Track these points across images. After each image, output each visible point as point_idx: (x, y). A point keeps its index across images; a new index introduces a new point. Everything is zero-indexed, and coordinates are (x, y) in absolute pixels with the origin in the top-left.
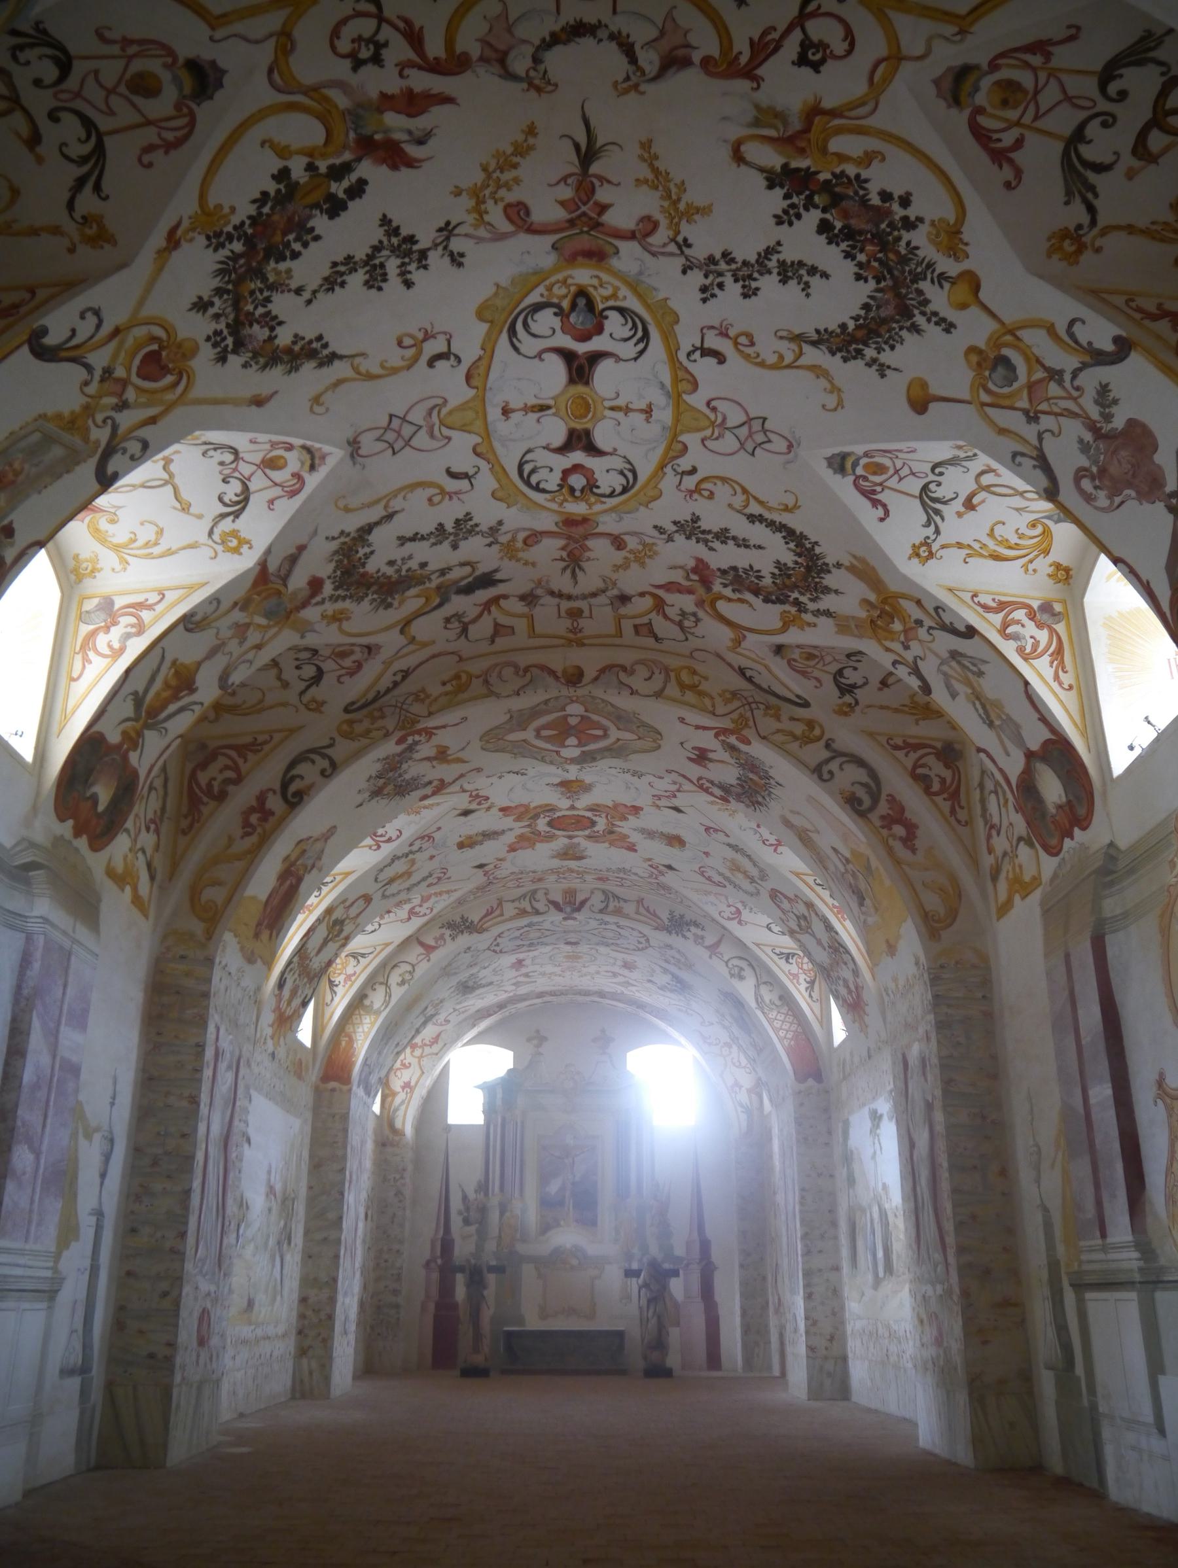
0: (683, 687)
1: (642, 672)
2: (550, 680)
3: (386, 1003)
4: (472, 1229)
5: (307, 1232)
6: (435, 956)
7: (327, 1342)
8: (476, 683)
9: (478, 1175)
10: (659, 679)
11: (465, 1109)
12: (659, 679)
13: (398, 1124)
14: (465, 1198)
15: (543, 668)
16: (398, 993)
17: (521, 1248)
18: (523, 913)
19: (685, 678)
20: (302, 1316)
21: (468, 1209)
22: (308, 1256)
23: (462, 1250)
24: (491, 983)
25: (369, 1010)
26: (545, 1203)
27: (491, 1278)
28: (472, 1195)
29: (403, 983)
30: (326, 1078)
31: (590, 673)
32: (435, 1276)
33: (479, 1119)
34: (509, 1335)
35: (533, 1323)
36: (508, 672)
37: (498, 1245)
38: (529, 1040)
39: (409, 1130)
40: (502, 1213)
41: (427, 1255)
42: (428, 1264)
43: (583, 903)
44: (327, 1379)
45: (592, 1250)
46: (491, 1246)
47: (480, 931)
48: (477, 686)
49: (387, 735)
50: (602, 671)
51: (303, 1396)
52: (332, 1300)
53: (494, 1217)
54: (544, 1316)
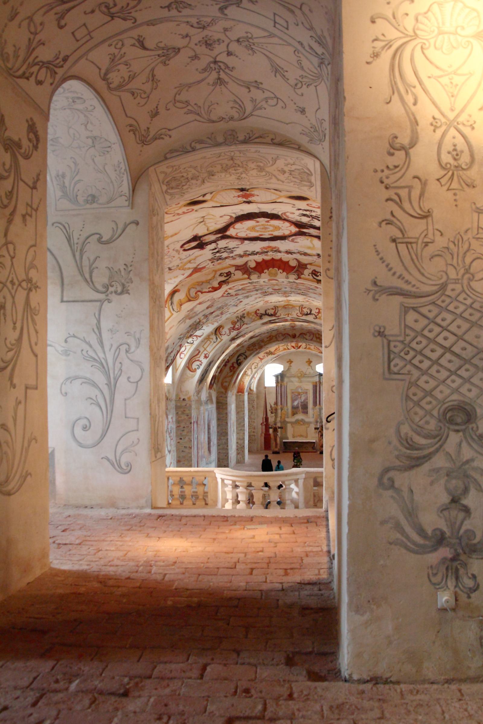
0: (317, 338)
1: (308, 334)
2: (289, 337)
3: (252, 373)
4: (274, 414)
5: (237, 428)
6: (263, 361)
7: (243, 451)
8: (274, 338)
9: (274, 400)
10: (312, 336)
11: (270, 382)
12: (312, 336)
13: (252, 388)
14: (271, 406)
15: (288, 334)
16: (254, 371)
17: (287, 420)
18: (285, 349)
19: (317, 336)
20: (237, 446)
22: (238, 433)
23: (271, 420)
25: (247, 375)
27: (279, 430)
28: (273, 406)
29: (255, 368)
30: (238, 392)
31: (297, 335)
32: (264, 427)
33: (274, 385)
34: (285, 443)
36: (280, 335)
38: (288, 362)
39: (255, 389)
40: (281, 411)
41: (261, 422)
42: (262, 424)
43: (300, 346)
44: (244, 459)
45: (307, 420)
46: (279, 419)
47: (274, 354)
48: (274, 338)
49: (257, 350)
50: (301, 334)
51: (239, 463)
52: (244, 443)
53: (279, 411)
54: (294, 437)
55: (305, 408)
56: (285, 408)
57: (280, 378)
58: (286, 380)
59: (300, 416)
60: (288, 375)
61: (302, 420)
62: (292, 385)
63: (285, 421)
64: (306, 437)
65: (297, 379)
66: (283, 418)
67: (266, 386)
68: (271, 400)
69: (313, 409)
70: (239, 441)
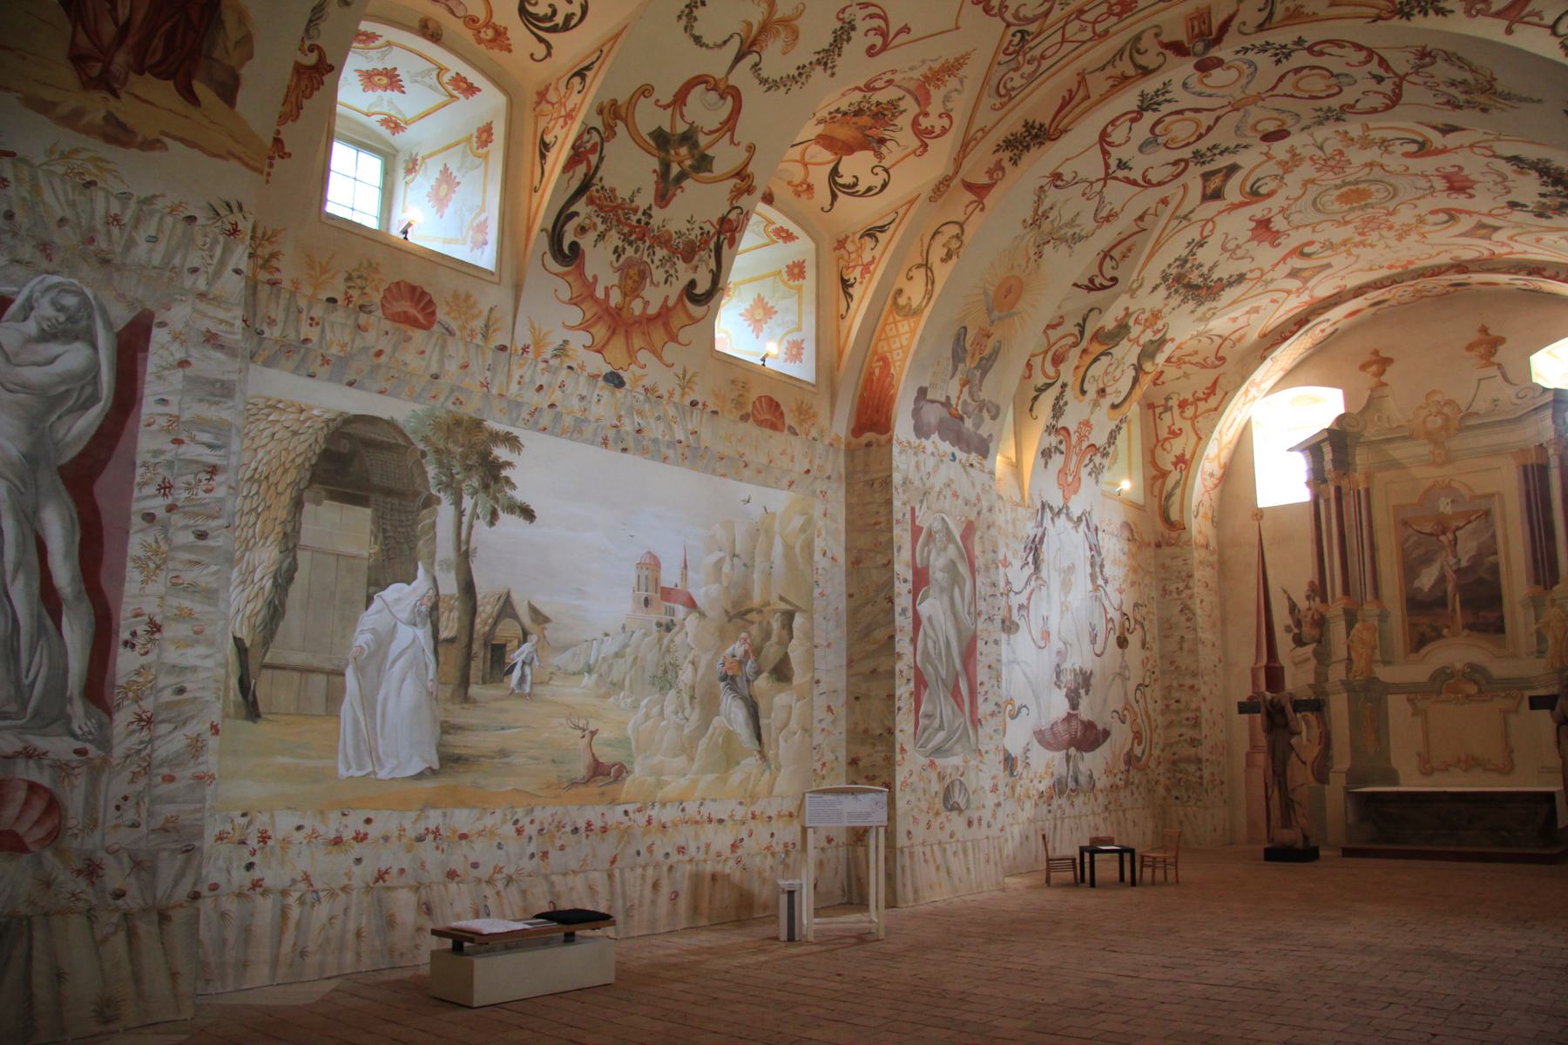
9: (1308, 572)
11: (1283, 483)
14: (1293, 607)
17: (1383, 673)
21: (1298, 624)
24: (1241, 278)
26: (1415, 604)
28: (1303, 604)
33: (1304, 495)
35: (1411, 783)
37: (1348, 670)
38: (1363, 367)
46: (1337, 673)
53: (1338, 630)
54: (1427, 771)
55: (1481, 600)
56: (1370, 609)
57: (1333, 452)
58: (1361, 459)
59: (1457, 651)
60: (1370, 434)
61: (1474, 673)
62: (1402, 480)
63: (1371, 681)
64: (1507, 769)
65: (1422, 449)
66: (1359, 664)
67: (1260, 505)
68: (1293, 575)
69: (1536, 603)
70: (863, 751)
